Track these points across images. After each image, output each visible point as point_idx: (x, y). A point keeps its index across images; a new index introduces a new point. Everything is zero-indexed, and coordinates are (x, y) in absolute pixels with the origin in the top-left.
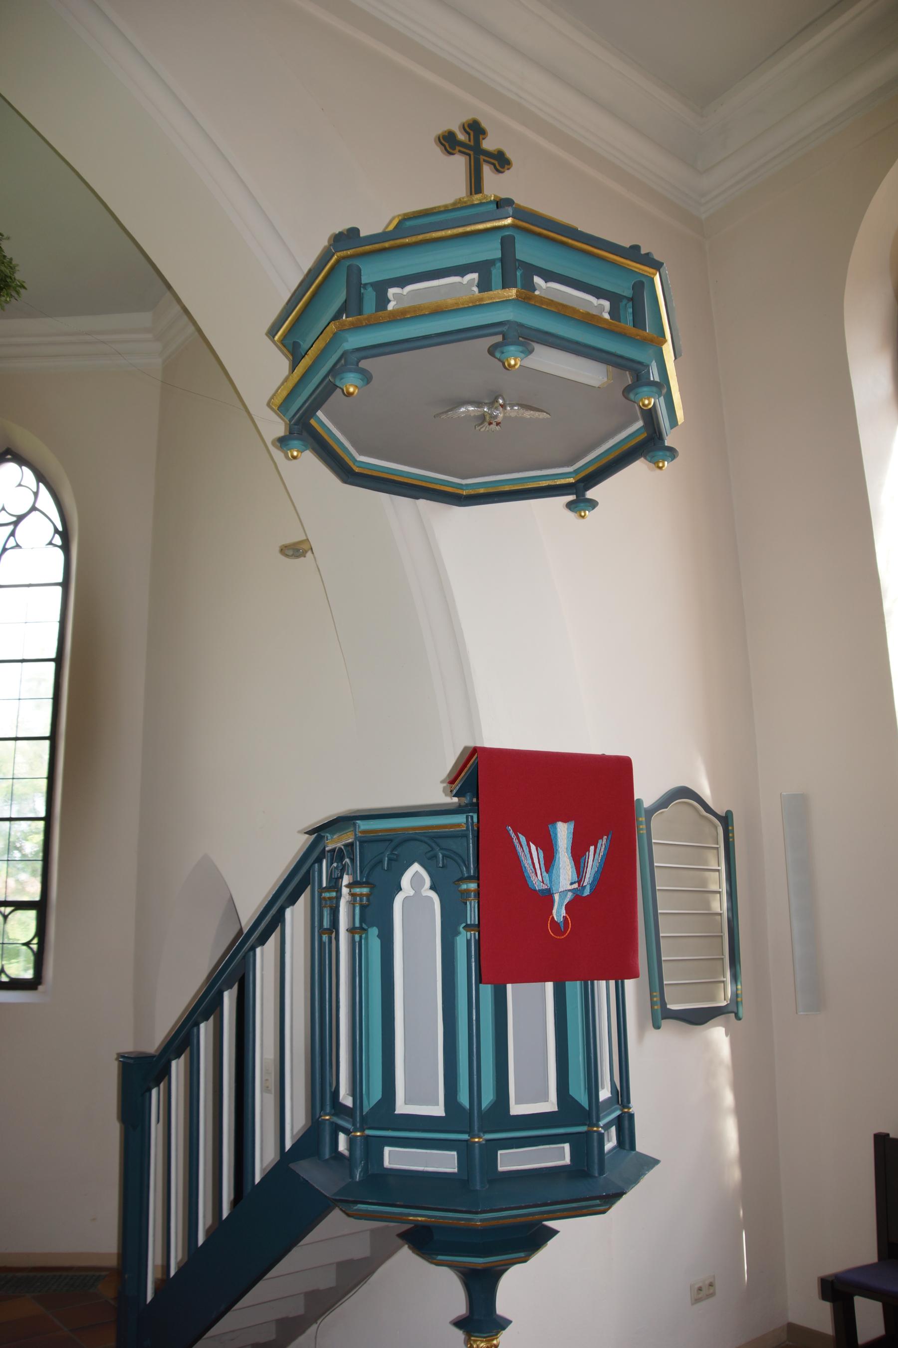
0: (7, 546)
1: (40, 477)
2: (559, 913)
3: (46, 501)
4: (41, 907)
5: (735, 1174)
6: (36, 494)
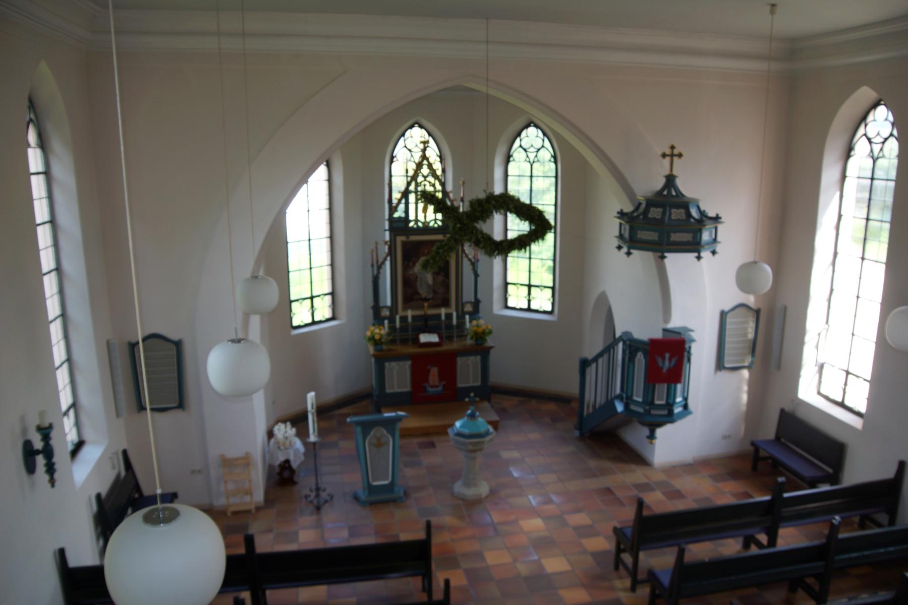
1: (545, 134)
2: (665, 370)
3: (547, 143)
5: (744, 408)
6: (543, 140)
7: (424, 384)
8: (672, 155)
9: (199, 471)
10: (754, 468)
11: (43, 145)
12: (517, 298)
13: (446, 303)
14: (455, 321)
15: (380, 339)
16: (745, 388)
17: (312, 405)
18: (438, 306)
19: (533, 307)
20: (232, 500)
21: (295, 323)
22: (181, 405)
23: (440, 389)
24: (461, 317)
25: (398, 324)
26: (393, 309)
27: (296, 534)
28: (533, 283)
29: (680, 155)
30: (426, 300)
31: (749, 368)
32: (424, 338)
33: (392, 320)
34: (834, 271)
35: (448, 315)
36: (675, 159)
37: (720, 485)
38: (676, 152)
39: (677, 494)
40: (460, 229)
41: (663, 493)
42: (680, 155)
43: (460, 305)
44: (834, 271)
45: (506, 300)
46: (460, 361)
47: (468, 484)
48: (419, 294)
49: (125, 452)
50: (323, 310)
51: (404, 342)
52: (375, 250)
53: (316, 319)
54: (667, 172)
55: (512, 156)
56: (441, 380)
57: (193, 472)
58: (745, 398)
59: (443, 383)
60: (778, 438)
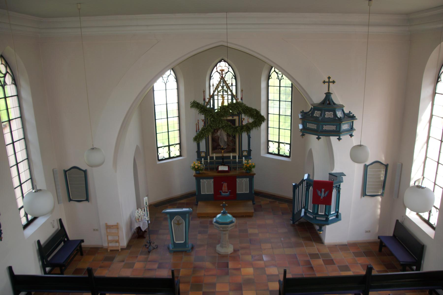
0: (282, 79)
2: (322, 198)
4: (290, 144)
5: (379, 217)
7: (220, 191)
8: (329, 82)
9: (97, 230)
10: (380, 250)
11: (15, 82)
12: (273, 148)
13: (234, 151)
14: (237, 160)
15: (198, 168)
16: (379, 206)
17: (146, 203)
18: (230, 152)
19: (281, 153)
20: (110, 245)
21: (160, 158)
22: (87, 200)
23: (228, 194)
24: (240, 157)
25: (209, 161)
26: (207, 153)
27: (134, 264)
28: (280, 141)
29: (334, 82)
30: (223, 149)
31: (382, 195)
32: (221, 168)
33: (206, 158)
34: (427, 147)
35: (234, 157)
36: (331, 84)
37: (357, 259)
38: (331, 80)
39: (329, 262)
40: (213, 121)
41: (323, 260)
42: (334, 82)
43: (241, 151)
44: (427, 147)
45: (268, 149)
46: (238, 180)
47: (222, 247)
48: (220, 146)
49: (60, 220)
50: (175, 151)
51: (212, 169)
52: (198, 124)
53: (172, 156)
54: (327, 91)
55: (271, 76)
56: (228, 190)
57: (94, 230)
58: (379, 211)
59: (229, 191)
60: (394, 235)
